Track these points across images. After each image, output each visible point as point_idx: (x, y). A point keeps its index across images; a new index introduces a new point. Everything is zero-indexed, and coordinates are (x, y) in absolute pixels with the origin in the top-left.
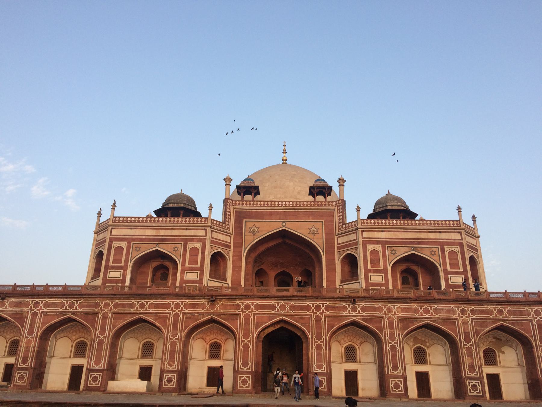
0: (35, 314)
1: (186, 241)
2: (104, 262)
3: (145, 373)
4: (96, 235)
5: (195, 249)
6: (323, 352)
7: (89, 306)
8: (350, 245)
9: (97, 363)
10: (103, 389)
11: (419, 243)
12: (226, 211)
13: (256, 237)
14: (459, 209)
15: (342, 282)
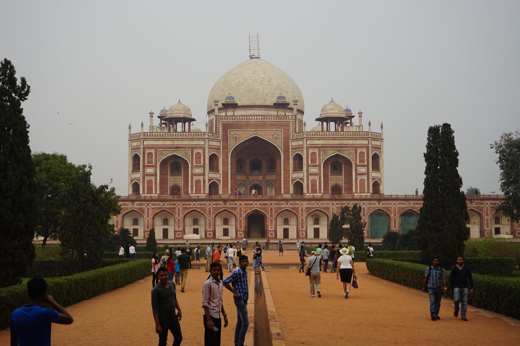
0: (148, 209)
1: (192, 148)
2: (141, 163)
3: (196, 231)
4: (130, 142)
5: (198, 153)
6: (274, 222)
7: (171, 205)
8: (299, 148)
9: (179, 228)
10: (182, 238)
11: (342, 147)
12: (216, 125)
13: (237, 142)
14: (370, 123)
15: (293, 171)
